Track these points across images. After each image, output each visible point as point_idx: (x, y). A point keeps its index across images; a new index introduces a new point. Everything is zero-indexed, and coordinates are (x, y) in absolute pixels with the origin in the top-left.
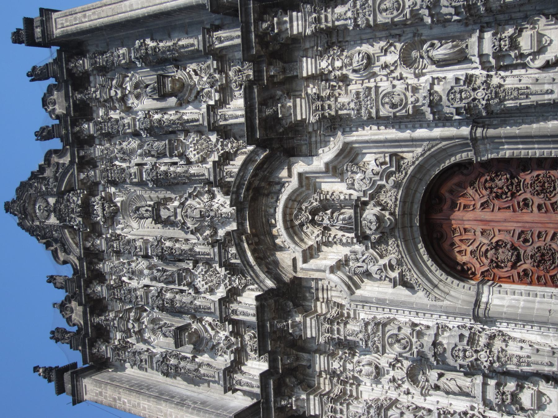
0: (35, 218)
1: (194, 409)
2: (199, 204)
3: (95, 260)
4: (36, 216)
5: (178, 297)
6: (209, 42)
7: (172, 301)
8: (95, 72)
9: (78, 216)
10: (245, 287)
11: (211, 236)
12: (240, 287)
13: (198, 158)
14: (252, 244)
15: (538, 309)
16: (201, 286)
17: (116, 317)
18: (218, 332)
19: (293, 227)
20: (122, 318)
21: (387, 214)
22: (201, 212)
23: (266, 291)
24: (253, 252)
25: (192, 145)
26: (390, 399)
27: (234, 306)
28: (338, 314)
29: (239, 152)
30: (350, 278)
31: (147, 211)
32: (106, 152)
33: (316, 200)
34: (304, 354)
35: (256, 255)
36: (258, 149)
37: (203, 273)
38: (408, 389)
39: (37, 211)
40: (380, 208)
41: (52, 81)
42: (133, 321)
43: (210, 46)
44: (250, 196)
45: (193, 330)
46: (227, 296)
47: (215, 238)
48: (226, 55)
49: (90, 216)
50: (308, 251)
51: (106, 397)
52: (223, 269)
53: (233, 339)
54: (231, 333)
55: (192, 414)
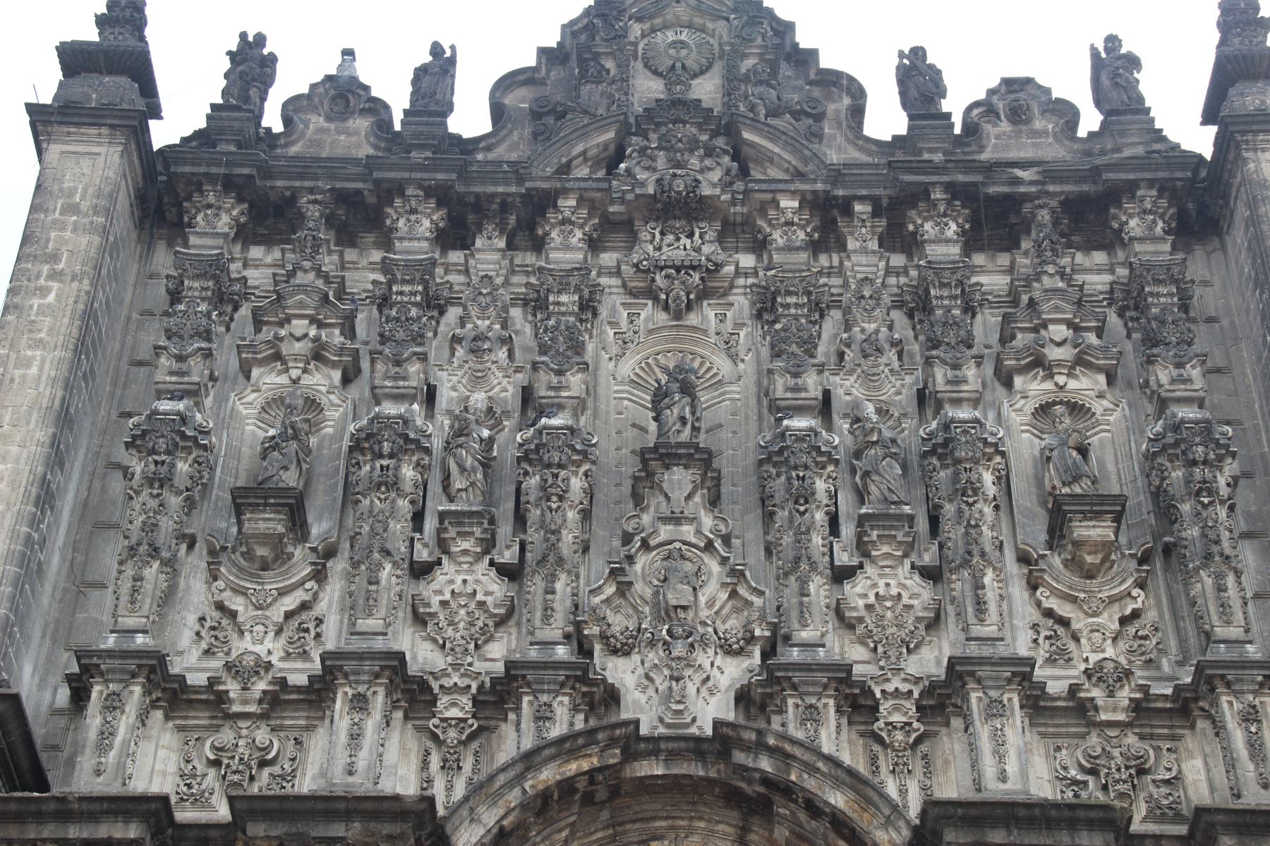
0: (647, 26)
1: (28, 541)
2: (711, 603)
3: (512, 220)
4: (653, 31)
5: (404, 505)
6: (1239, 681)
7: (390, 484)
8: (1123, 272)
9: (659, 181)
10: (435, 737)
11: (604, 637)
12: (435, 721)
13: (855, 609)
14: (592, 781)
16: (435, 586)
17: (326, 278)
18: (279, 632)
22: (685, 608)
23: (443, 827)
24: (566, 787)
25: (894, 591)
27: (379, 700)
29: (877, 748)
31: (683, 420)
32: (867, 293)
36: (906, 833)
37: (479, 597)
39: (670, 36)
41: (1090, 120)
42: (317, 339)
43: (1228, 685)
44: (743, 785)
45: (290, 549)
46: (407, 679)
47: (597, 648)
48: (1192, 727)
49: (657, 219)
52: (499, 668)
53: (261, 686)
54: (283, 682)
55: (13, 534)
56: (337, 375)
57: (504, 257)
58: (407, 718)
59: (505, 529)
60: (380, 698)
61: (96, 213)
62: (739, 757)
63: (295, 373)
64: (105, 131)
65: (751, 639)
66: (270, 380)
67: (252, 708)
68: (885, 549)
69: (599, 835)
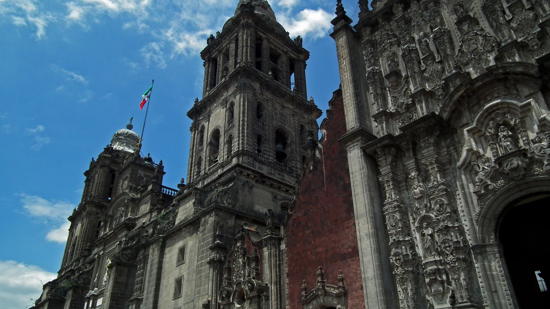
5: (415, 62)
11: (462, 64)
15: (495, 284)
19: (490, 114)
20: (388, 34)
21: (523, 173)
22: (475, 49)
24: (462, 97)
25: (523, 18)
26: (406, 210)
28: (444, 164)
29: (532, 52)
30: (470, 163)
33: (515, 122)
34: (412, 153)
35: (460, 99)
38: (416, 219)
40: (525, 167)
42: (390, 42)
47: (462, 66)
50: (477, 130)
51: (341, 51)
53: (404, 106)
54: (407, 104)
56: (396, 46)
57: (417, 5)
58: (432, 98)
59: (436, 55)
60: (423, 98)
61: (346, 45)
62: (495, 72)
63: (389, 50)
64: (342, 31)
65: (493, 47)
66: (386, 54)
67: (404, 111)
68: (517, 10)
69: (475, 101)
